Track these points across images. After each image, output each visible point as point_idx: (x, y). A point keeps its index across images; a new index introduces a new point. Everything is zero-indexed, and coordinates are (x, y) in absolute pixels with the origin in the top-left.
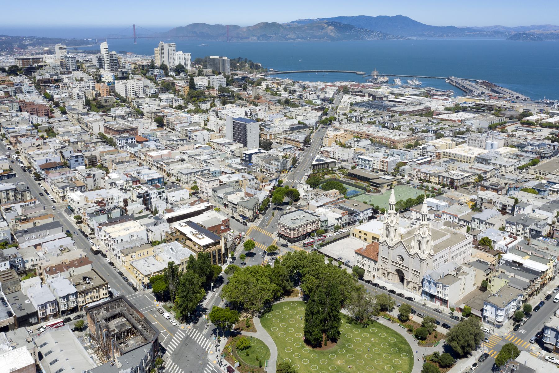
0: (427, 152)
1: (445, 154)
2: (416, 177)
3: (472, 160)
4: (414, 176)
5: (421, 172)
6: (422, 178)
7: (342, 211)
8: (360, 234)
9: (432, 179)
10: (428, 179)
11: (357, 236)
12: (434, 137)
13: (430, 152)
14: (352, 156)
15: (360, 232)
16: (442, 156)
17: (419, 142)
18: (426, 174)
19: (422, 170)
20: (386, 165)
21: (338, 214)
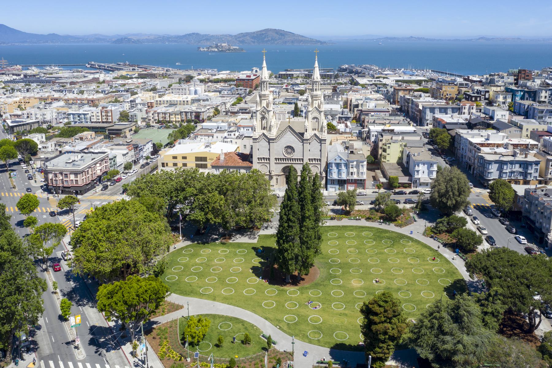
0: (137, 104)
1: (159, 102)
2: (152, 120)
3: (190, 103)
4: (150, 120)
5: (158, 113)
6: (161, 119)
7: (126, 147)
8: (175, 161)
9: (173, 118)
10: (168, 120)
11: (170, 164)
12: (130, 95)
13: (140, 104)
14: (55, 115)
15: (175, 158)
16: (155, 105)
17: (119, 99)
18: (165, 114)
19: (159, 111)
20: (110, 114)
21: (124, 150)
